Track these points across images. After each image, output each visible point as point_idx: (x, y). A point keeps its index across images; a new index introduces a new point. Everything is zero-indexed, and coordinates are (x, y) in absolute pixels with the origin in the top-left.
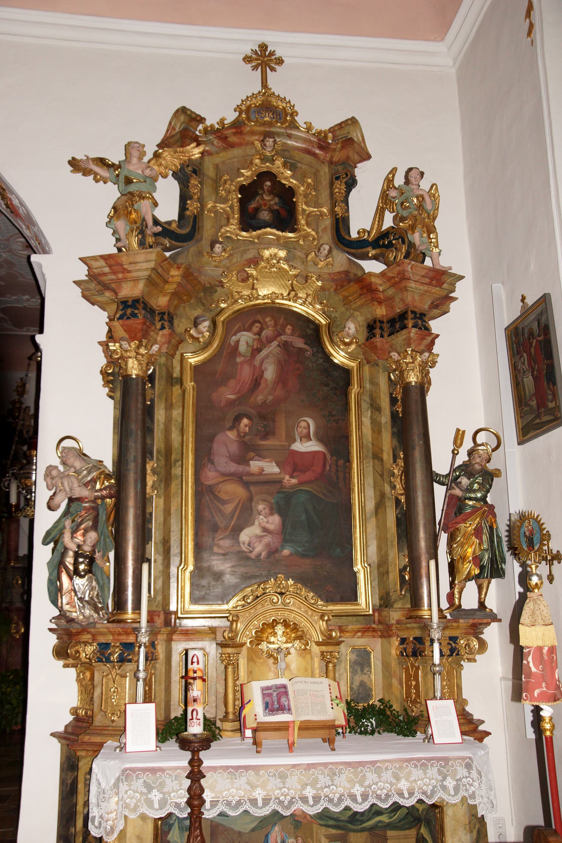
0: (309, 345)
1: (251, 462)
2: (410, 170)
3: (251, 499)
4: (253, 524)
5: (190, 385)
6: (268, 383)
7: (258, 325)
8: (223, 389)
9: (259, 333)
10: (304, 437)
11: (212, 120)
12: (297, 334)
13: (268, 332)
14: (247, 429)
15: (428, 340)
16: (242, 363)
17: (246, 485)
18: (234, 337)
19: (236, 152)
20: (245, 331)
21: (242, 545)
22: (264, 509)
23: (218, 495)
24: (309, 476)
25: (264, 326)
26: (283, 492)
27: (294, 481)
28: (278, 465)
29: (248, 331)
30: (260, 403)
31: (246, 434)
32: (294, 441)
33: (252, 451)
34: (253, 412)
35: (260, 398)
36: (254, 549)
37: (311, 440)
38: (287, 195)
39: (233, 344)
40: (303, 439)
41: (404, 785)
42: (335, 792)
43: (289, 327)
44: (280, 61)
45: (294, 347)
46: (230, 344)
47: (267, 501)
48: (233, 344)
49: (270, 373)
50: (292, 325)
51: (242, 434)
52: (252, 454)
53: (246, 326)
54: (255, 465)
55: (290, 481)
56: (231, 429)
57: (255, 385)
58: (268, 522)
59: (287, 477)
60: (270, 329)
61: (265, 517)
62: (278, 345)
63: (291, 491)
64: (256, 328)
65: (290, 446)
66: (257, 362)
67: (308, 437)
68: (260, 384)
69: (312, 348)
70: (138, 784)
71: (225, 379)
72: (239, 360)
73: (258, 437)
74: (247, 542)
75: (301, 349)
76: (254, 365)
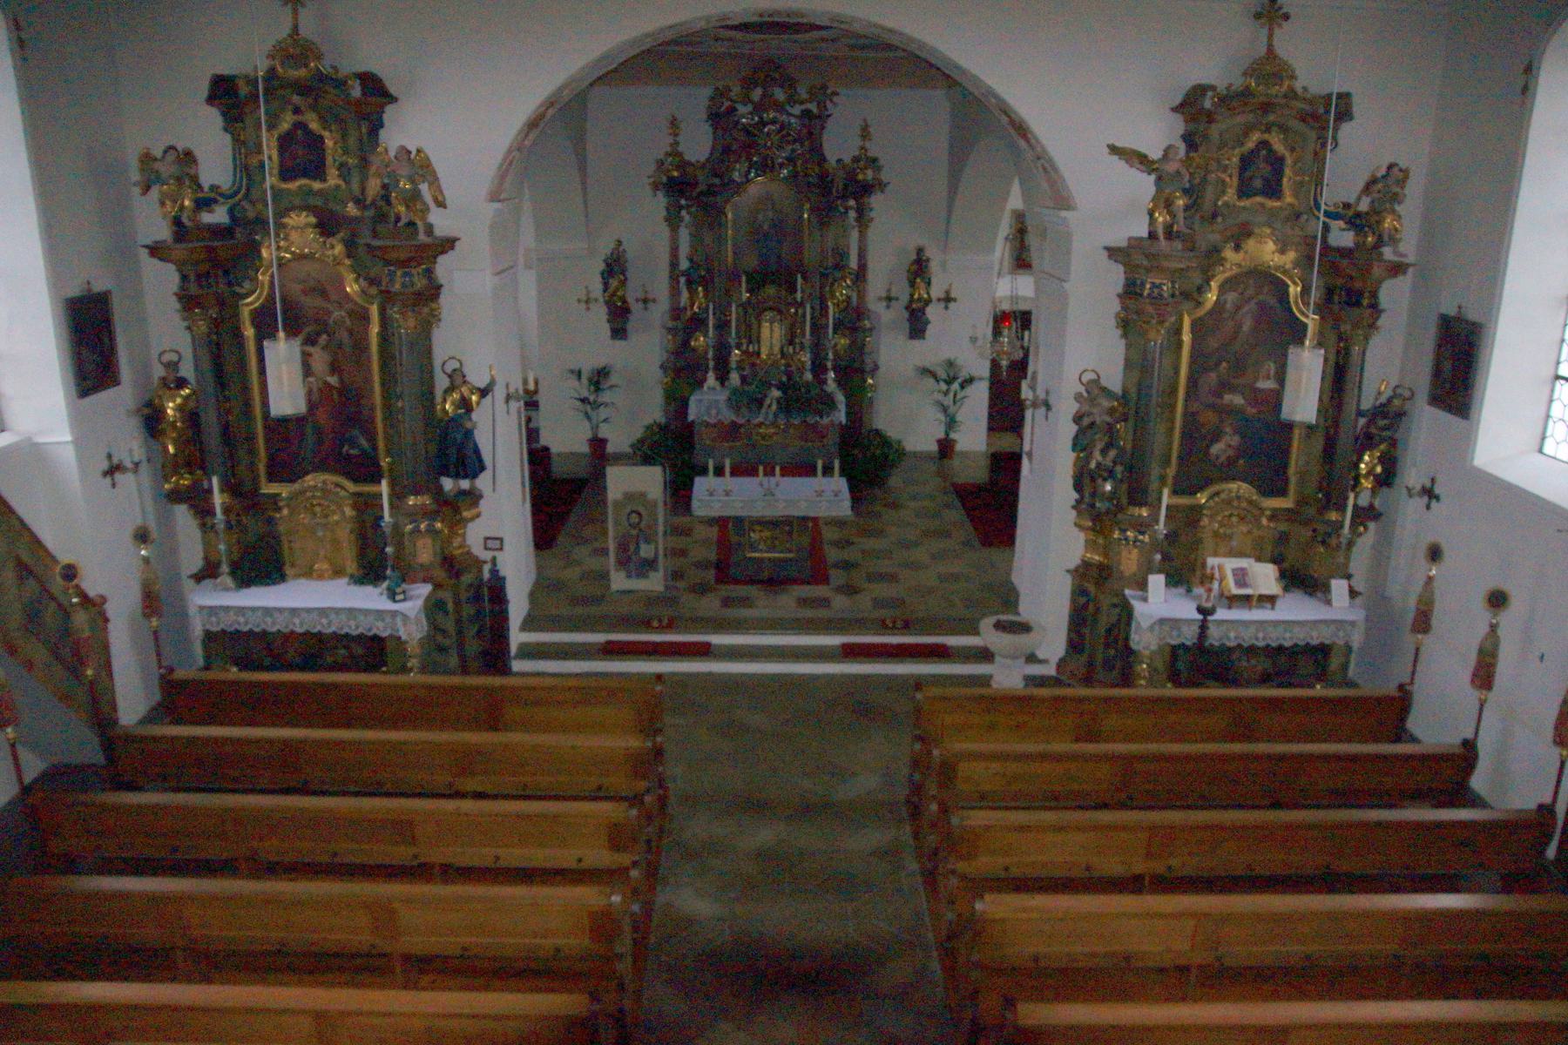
2: (1390, 167)
5: (1186, 337)
11: (1221, 86)
19: (1239, 119)
38: (1277, 163)
42: (1273, 635)
44: (1286, 17)
49: (1247, 325)
54: (1228, 398)
55: (1251, 411)
72: (1225, 315)
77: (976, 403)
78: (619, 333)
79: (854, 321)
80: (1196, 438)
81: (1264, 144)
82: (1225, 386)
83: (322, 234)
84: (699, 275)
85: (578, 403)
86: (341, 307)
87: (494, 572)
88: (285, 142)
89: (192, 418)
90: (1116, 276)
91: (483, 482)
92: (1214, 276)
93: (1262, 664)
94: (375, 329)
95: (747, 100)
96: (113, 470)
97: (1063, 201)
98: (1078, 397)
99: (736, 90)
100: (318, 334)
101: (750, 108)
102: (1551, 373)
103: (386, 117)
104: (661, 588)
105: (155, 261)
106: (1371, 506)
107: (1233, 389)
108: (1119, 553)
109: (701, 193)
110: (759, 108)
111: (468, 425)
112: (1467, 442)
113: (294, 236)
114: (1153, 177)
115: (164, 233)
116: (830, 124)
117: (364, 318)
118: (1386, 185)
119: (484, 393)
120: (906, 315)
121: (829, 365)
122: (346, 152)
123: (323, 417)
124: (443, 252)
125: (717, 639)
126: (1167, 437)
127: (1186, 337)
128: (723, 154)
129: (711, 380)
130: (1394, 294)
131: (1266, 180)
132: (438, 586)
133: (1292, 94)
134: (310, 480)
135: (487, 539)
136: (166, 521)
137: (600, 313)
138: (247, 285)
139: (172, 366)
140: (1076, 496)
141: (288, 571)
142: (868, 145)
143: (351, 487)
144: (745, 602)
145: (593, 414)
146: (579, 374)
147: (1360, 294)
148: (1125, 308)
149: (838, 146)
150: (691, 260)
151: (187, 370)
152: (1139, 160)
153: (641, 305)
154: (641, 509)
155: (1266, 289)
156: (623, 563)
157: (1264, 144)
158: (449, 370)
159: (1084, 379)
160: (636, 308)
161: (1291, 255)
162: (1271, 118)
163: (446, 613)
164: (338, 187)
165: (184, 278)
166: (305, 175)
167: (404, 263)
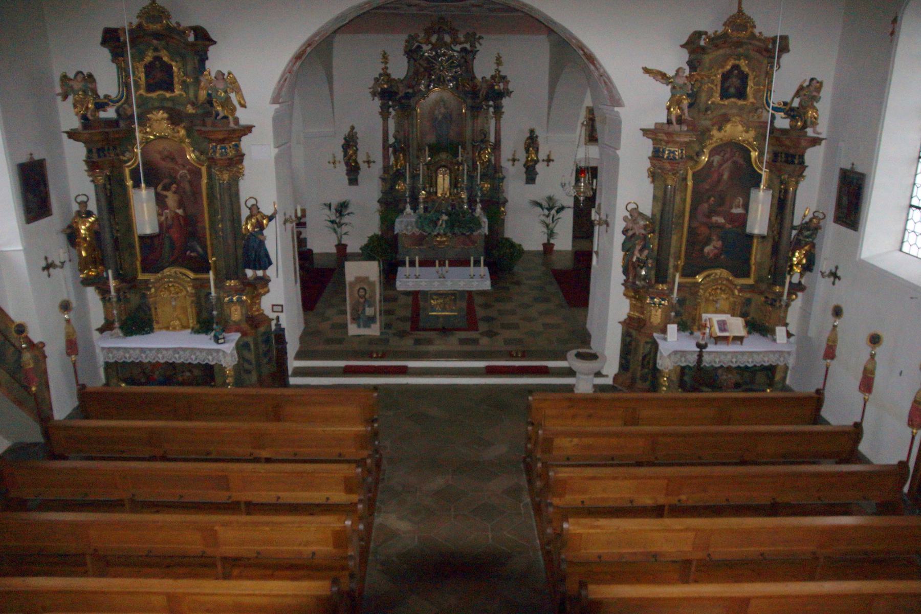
2: (812, 80)
5: (690, 183)
11: (711, 32)
13: (727, 155)
15: (802, 166)
17: (710, 228)
19: (721, 52)
35: (720, 188)
38: (744, 78)
41: (766, 359)
49: (725, 177)
54: (714, 219)
55: (728, 226)
70: (678, 356)
77: (566, 220)
78: (353, 181)
79: (494, 173)
80: (695, 242)
81: (736, 67)
82: (712, 212)
83: (172, 124)
84: (399, 147)
85: (329, 224)
86: (184, 166)
87: (278, 325)
88: (149, 68)
89: (95, 233)
90: (647, 147)
91: (271, 272)
93: (734, 378)
94: (204, 181)
95: (428, 42)
96: (48, 267)
97: (618, 102)
98: (625, 219)
99: (422, 35)
100: (171, 184)
101: (430, 46)
102: (907, 203)
103: (210, 54)
104: (378, 333)
105: (71, 141)
106: (800, 282)
107: (718, 214)
108: (651, 311)
109: (402, 98)
110: (434, 47)
111: (262, 238)
112: (856, 245)
113: (155, 125)
114: (670, 87)
115: (75, 123)
116: (478, 56)
117: (198, 173)
118: (809, 92)
119: (270, 218)
120: (524, 170)
121: (478, 200)
122: (186, 74)
123: (175, 233)
124: (245, 134)
125: (412, 364)
126: (678, 242)
127: (690, 183)
128: (414, 76)
129: (408, 209)
130: (814, 157)
131: (737, 89)
132: (244, 334)
133: (753, 36)
134: (167, 271)
135: (273, 305)
136: (82, 298)
137: (342, 168)
138: (128, 155)
139: (84, 204)
140: (624, 278)
141: (155, 326)
142: (500, 68)
143: (192, 275)
144: (430, 342)
145: (339, 230)
146: (330, 206)
147: (793, 156)
148: (653, 165)
149: (483, 69)
150: (395, 137)
151: (92, 206)
152: (662, 76)
153: (366, 165)
154: (366, 287)
156: (356, 319)
157: (736, 67)
158: (249, 205)
159: (629, 208)
160: (363, 166)
161: (752, 133)
162: (740, 50)
163: (249, 350)
164: (181, 95)
165: (90, 151)
166: (161, 89)
167: (222, 141)
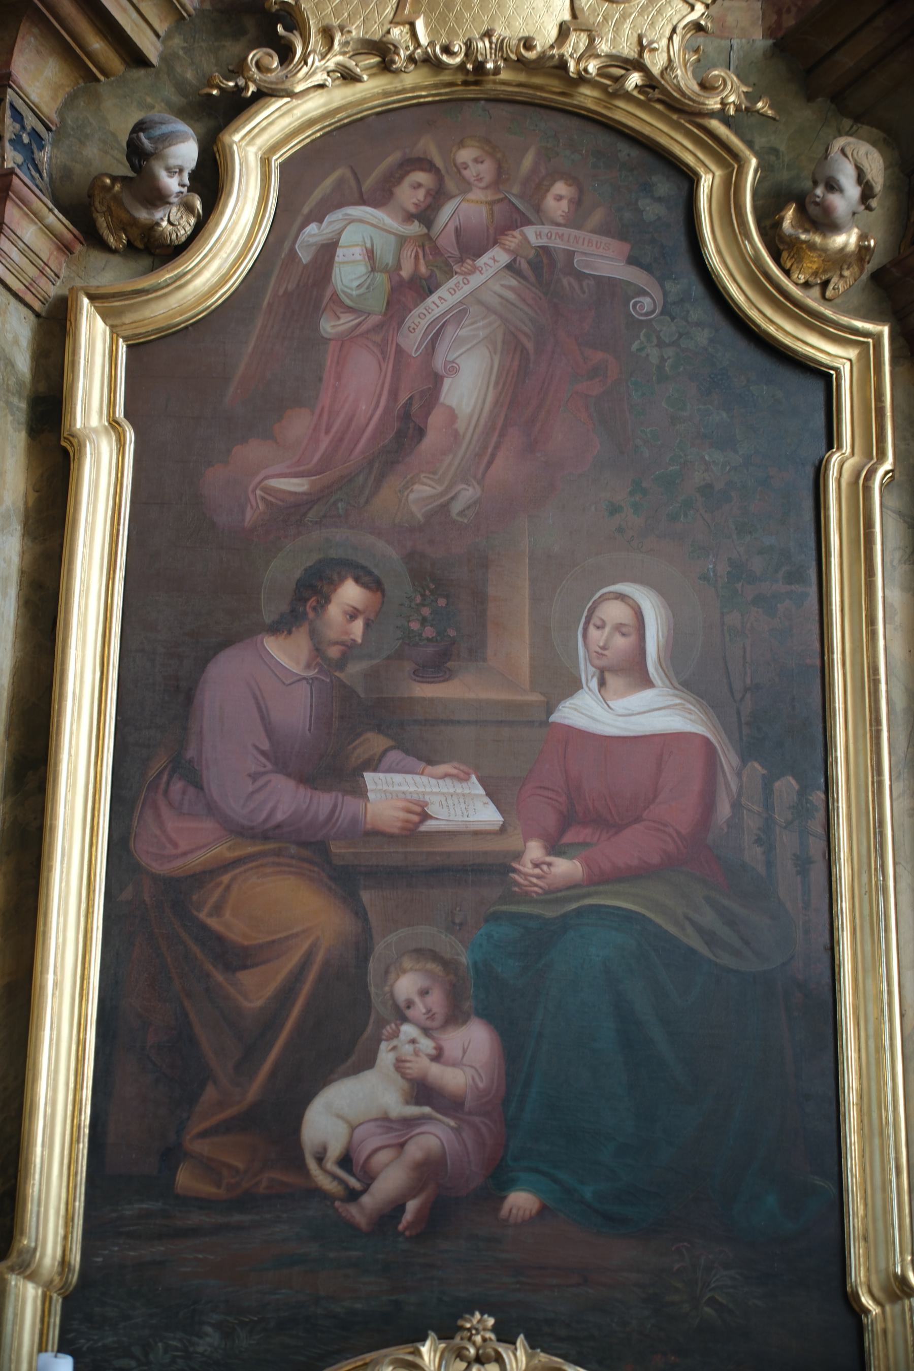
0: (647, 268)
1: (369, 776)
3: (362, 948)
4: (368, 1062)
6: (460, 425)
7: (421, 177)
8: (252, 451)
9: (425, 216)
10: (616, 670)
12: (597, 217)
13: (465, 210)
14: (358, 627)
16: (346, 340)
18: (312, 228)
20: (362, 201)
21: (312, 1165)
22: (424, 993)
23: (213, 923)
24: (631, 846)
25: (450, 185)
26: (513, 917)
27: (565, 868)
28: (492, 794)
29: (376, 203)
30: (419, 513)
31: (350, 650)
32: (574, 686)
33: (379, 728)
34: (386, 553)
35: (422, 493)
36: (369, 1178)
37: (646, 682)
39: (305, 256)
40: (610, 679)
43: (560, 188)
45: (580, 276)
46: (292, 253)
47: (435, 956)
48: (305, 256)
49: (468, 386)
50: (571, 179)
51: (334, 652)
52: (375, 742)
53: (368, 184)
54: (390, 792)
56: (282, 626)
57: (400, 435)
58: (438, 1057)
59: (535, 850)
60: (477, 194)
61: (426, 1031)
62: (509, 267)
63: (550, 913)
64: (412, 191)
65: (550, 709)
66: (412, 340)
67: (636, 673)
68: (421, 432)
69: (661, 281)
71: (266, 411)
72: (329, 326)
73: (408, 666)
74: (335, 1150)
75: (609, 290)
76: (399, 351)
82: (361, 721)
92: (236, 106)
107: (420, 740)
155: (559, 198)
